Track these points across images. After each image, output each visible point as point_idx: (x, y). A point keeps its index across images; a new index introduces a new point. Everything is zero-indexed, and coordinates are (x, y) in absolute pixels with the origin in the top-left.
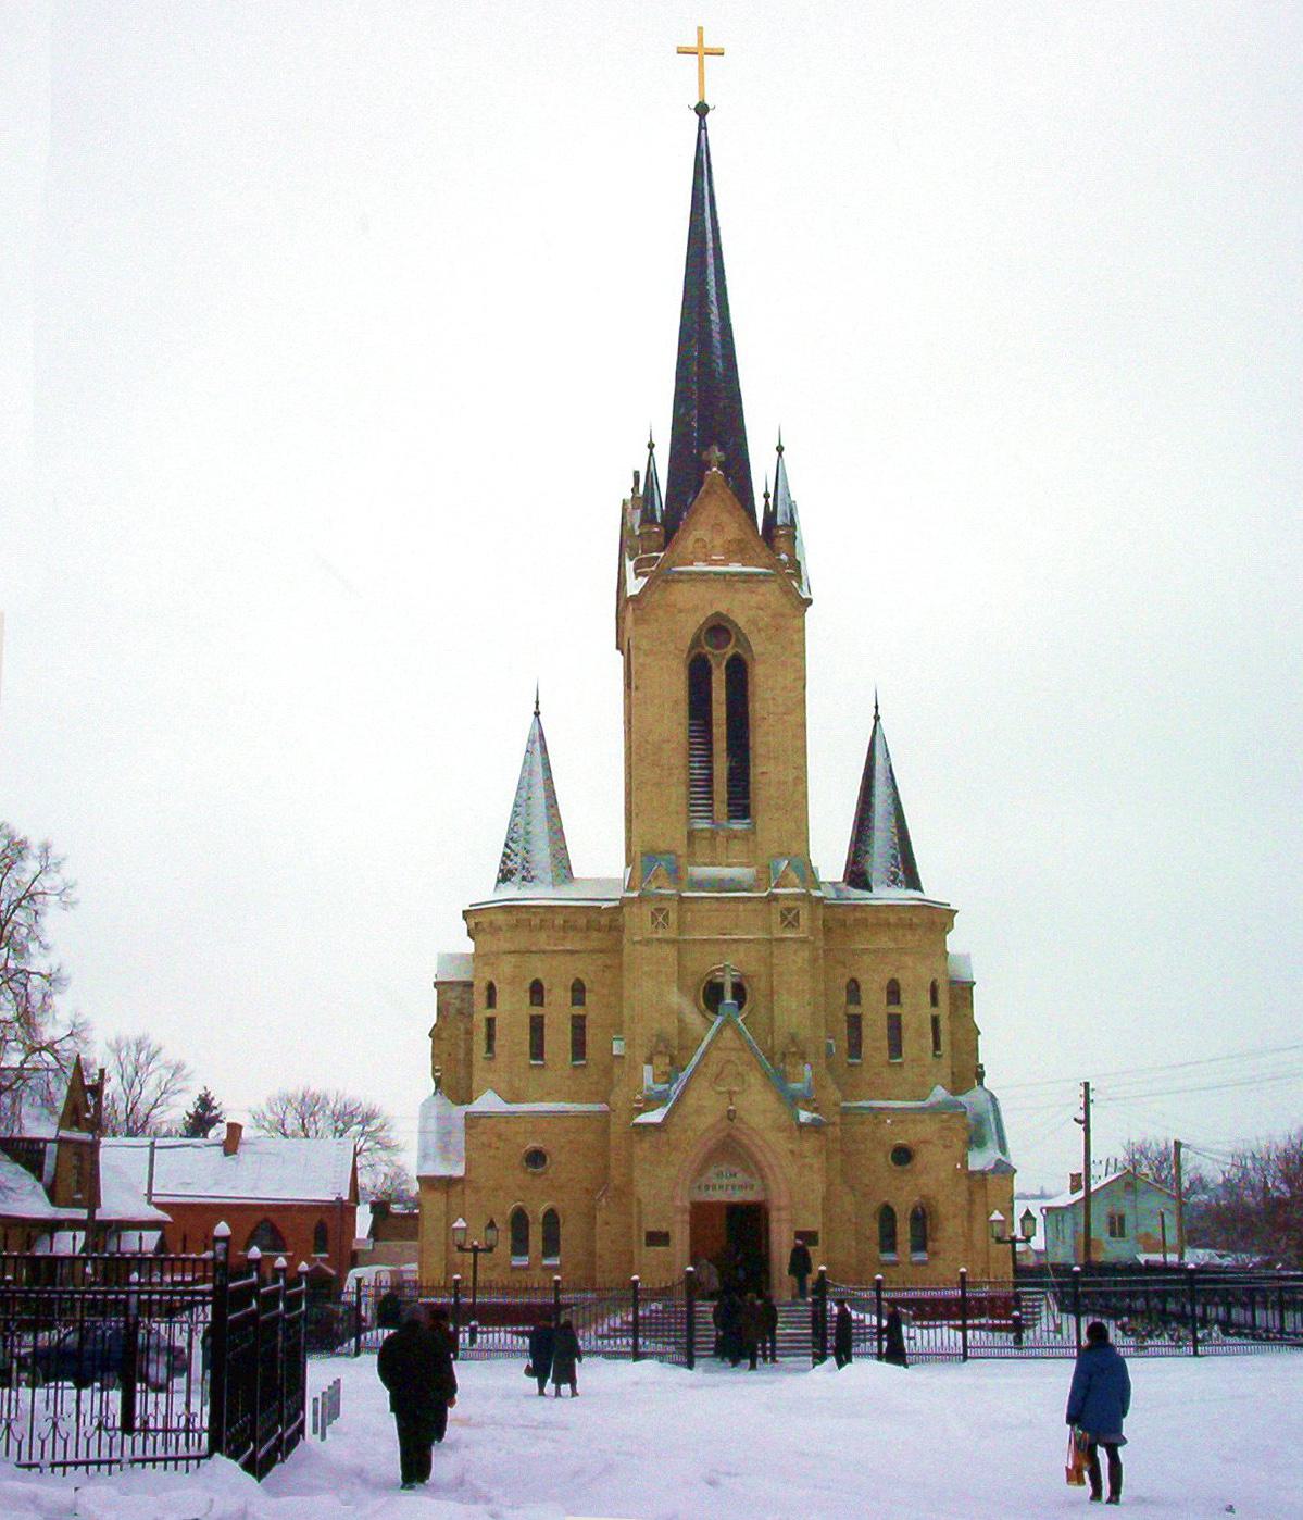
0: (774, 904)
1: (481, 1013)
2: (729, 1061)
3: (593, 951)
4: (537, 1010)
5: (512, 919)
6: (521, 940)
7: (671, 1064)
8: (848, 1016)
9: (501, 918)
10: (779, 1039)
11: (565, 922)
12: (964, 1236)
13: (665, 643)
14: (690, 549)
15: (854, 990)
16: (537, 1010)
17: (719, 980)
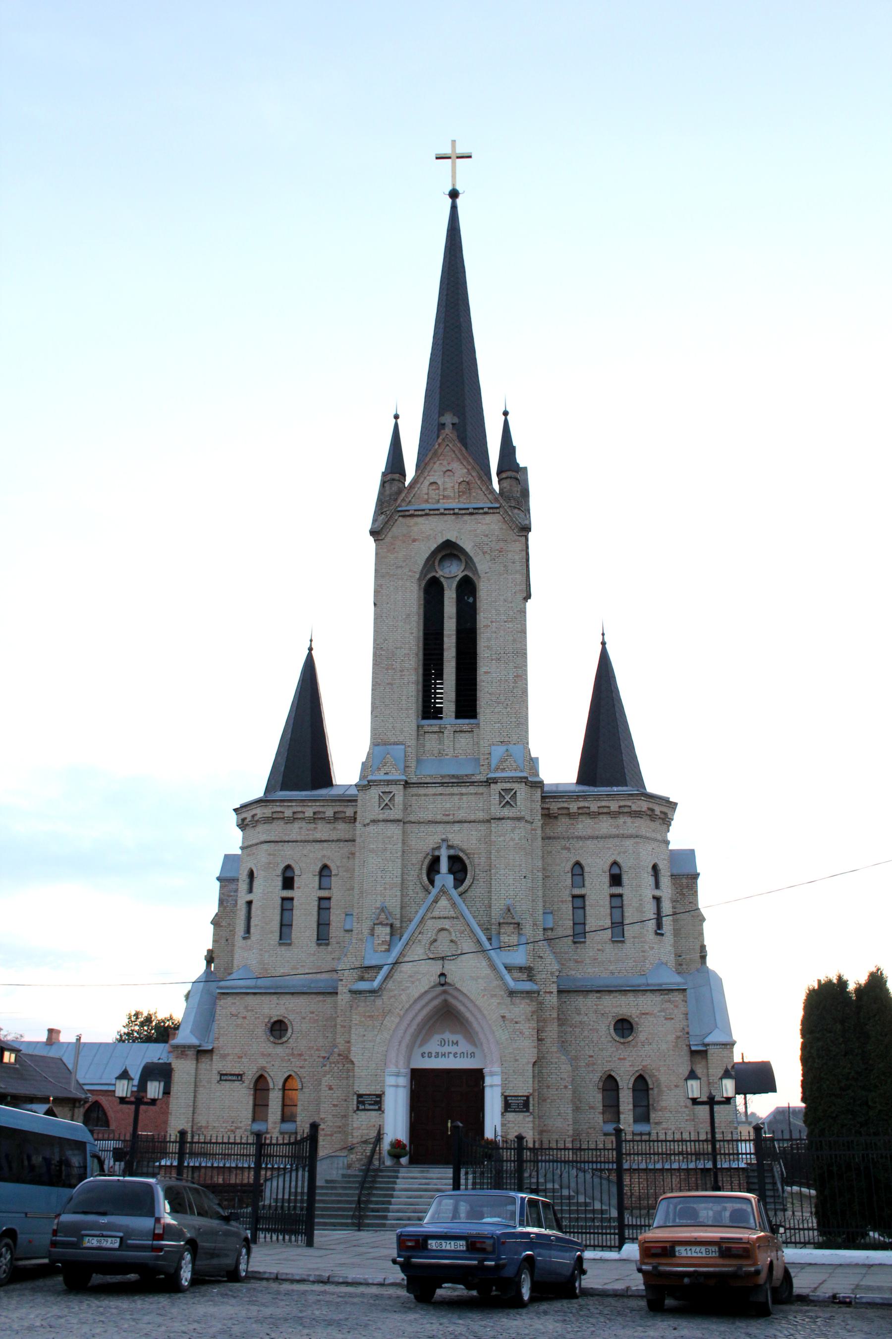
0: (492, 785)
1: (243, 897)
2: (443, 929)
3: (338, 841)
4: (287, 893)
5: (267, 811)
6: (276, 831)
7: (392, 934)
8: (574, 897)
9: (259, 812)
10: (496, 913)
11: (314, 813)
12: (686, 1107)
13: (401, 567)
14: (425, 490)
15: (578, 869)
16: (287, 893)
17: (437, 853)
